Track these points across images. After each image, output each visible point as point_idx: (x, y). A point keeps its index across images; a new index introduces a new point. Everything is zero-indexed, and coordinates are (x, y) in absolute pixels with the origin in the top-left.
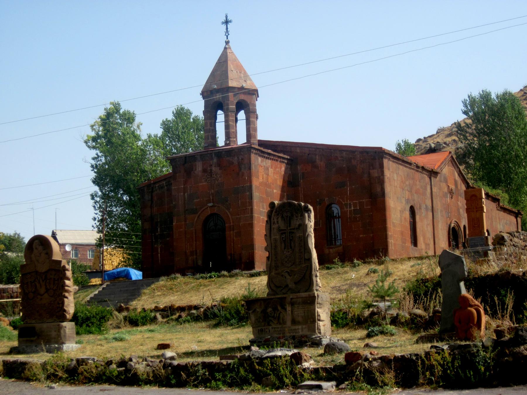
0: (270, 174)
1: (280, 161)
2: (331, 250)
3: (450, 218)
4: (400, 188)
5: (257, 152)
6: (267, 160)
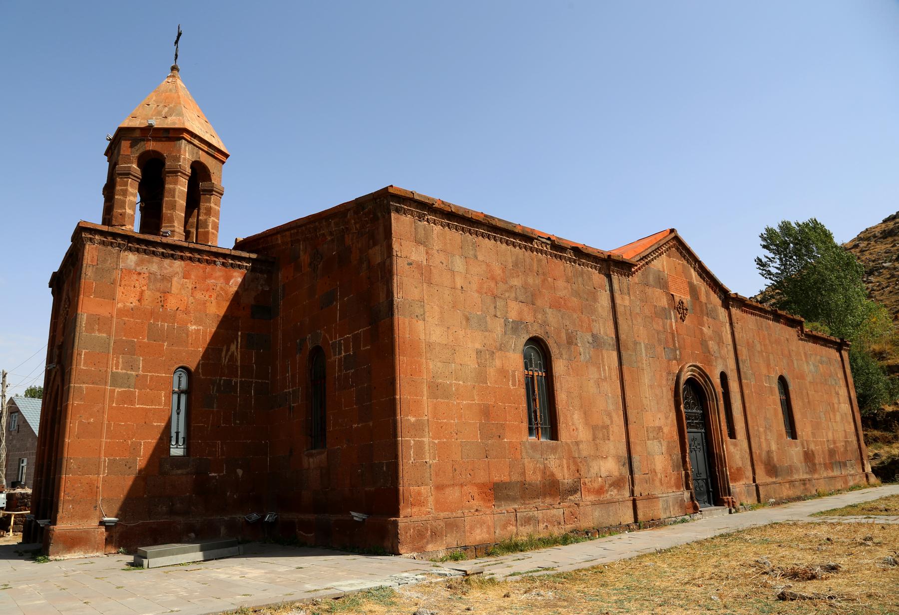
0: (174, 290)
1: (223, 264)
2: (311, 460)
3: (679, 361)
4: (478, 292)
5: (110, 239)
6: (167, 262)
